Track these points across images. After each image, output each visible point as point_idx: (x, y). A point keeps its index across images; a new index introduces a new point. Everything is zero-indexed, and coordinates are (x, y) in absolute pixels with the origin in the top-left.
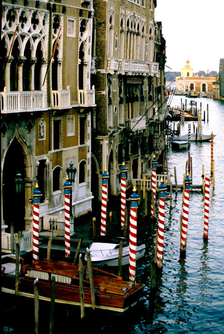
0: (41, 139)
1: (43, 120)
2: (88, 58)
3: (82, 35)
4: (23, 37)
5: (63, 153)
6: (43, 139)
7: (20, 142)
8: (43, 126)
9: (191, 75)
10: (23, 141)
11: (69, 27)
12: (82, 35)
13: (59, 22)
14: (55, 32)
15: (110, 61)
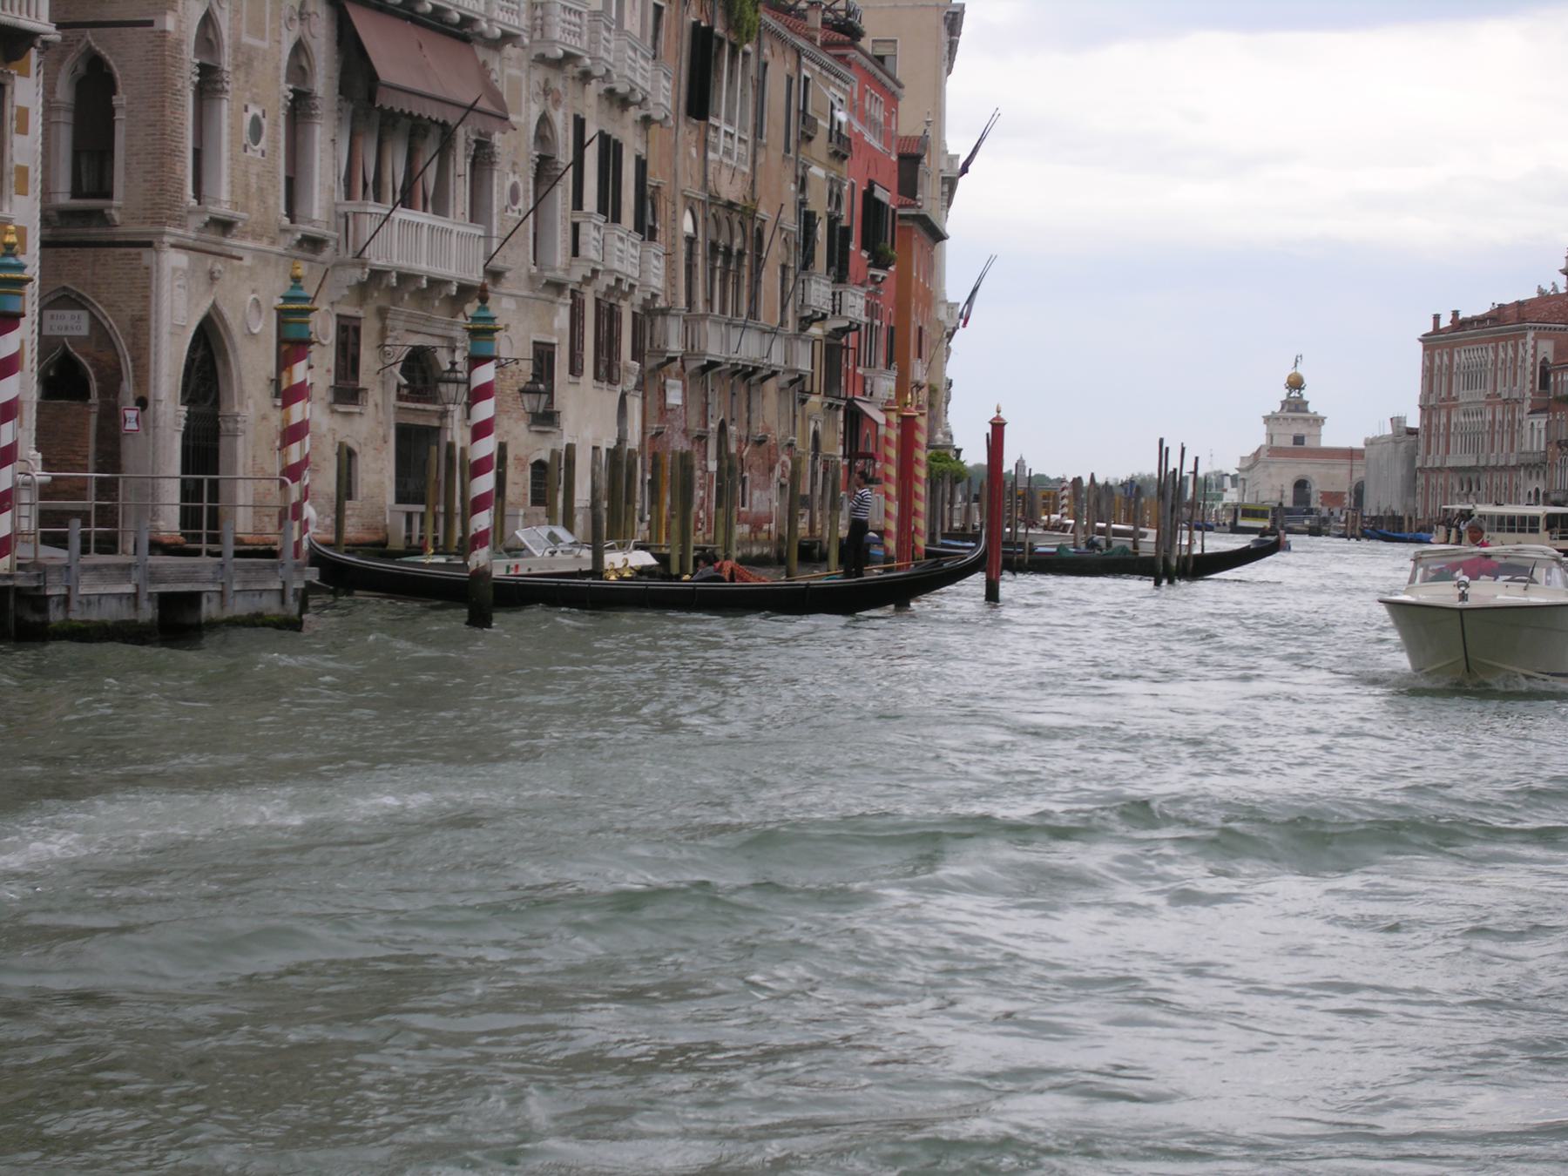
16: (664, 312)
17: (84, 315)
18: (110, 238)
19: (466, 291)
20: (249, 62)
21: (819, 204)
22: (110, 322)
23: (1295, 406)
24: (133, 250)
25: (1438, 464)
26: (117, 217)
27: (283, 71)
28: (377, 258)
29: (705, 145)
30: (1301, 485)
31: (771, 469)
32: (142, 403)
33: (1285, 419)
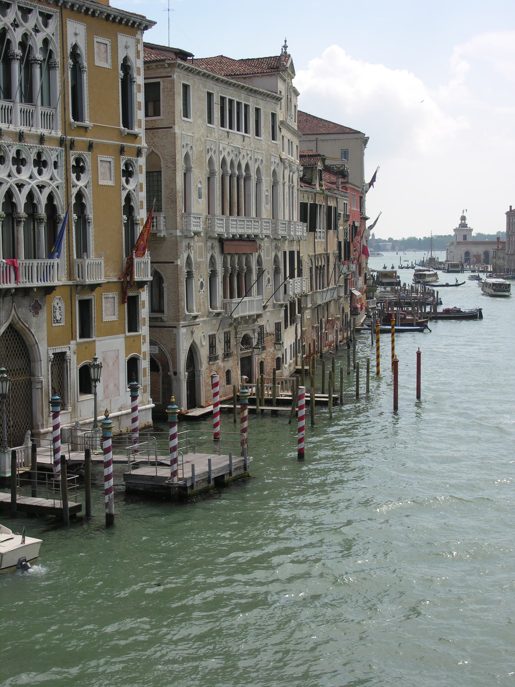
0: (57, 325)
1: (60, 299)
2: (141, 215)
3: (127, 182)
4: (20, 186)
5: (97, 343)
6: (60, 324)
7: (20, 328)
8: (60, 307)
9: (469, 239)
10: (26, 326)
11: (103, 171)
12: (127, 182)
13: (84, 163)
14: (78, 178)
15: (156, 219)
16: (306, 296)
17: (157, 347)
18: (164, 325)
19: (259, 316)
20: (199, 267)
21: (341, 239)
22: (164, 349)
23: (463, 225)
24: (171, 329)
25: (512, 253)
26: (165, 319)
27: (208, 266)
28: (235, 316)
29: (315, 238)
30: (467, 254)
31: (333, 327)
32: (175, 373)
33: (460, 230)
